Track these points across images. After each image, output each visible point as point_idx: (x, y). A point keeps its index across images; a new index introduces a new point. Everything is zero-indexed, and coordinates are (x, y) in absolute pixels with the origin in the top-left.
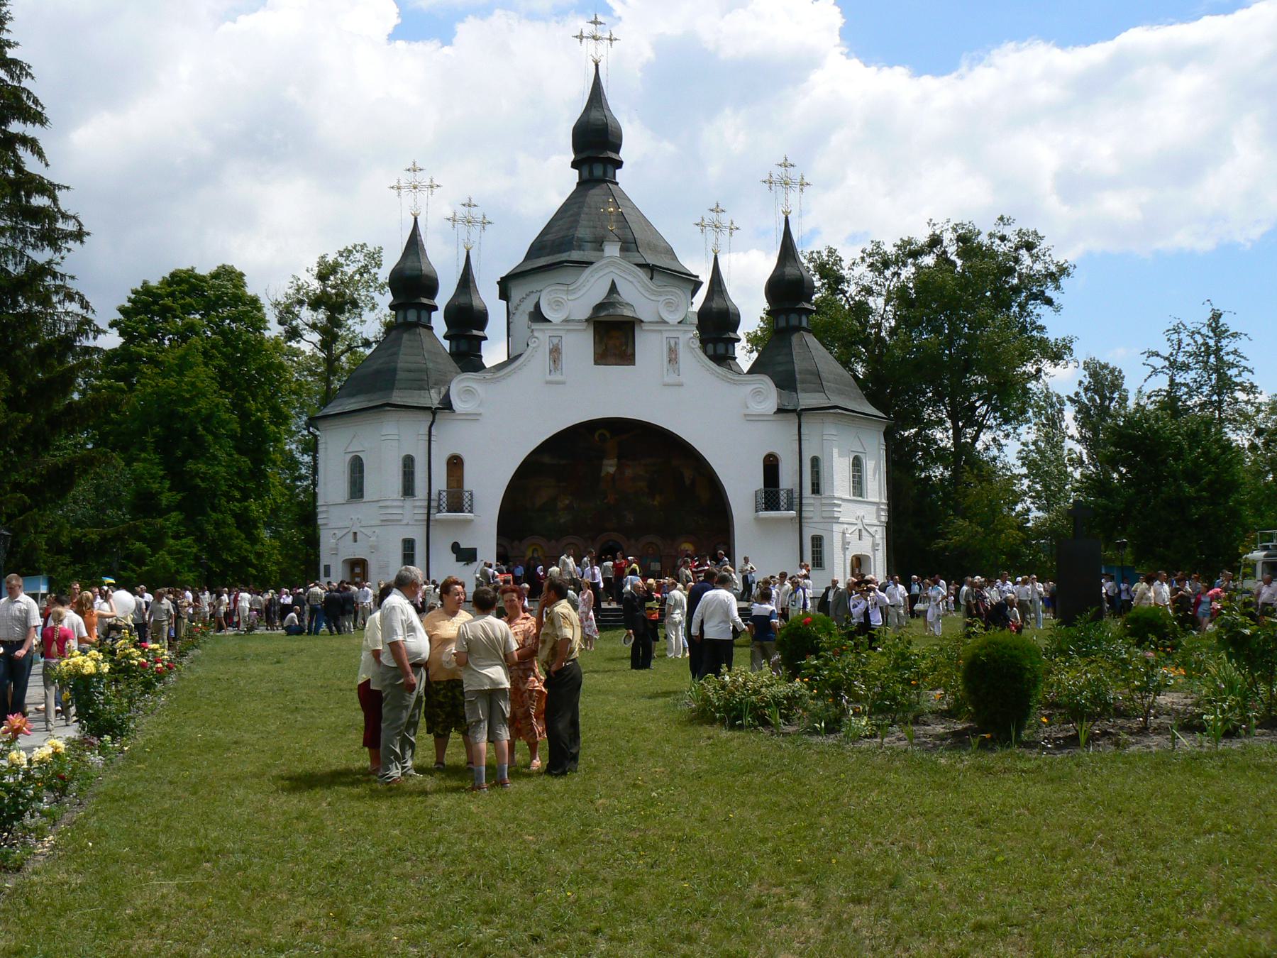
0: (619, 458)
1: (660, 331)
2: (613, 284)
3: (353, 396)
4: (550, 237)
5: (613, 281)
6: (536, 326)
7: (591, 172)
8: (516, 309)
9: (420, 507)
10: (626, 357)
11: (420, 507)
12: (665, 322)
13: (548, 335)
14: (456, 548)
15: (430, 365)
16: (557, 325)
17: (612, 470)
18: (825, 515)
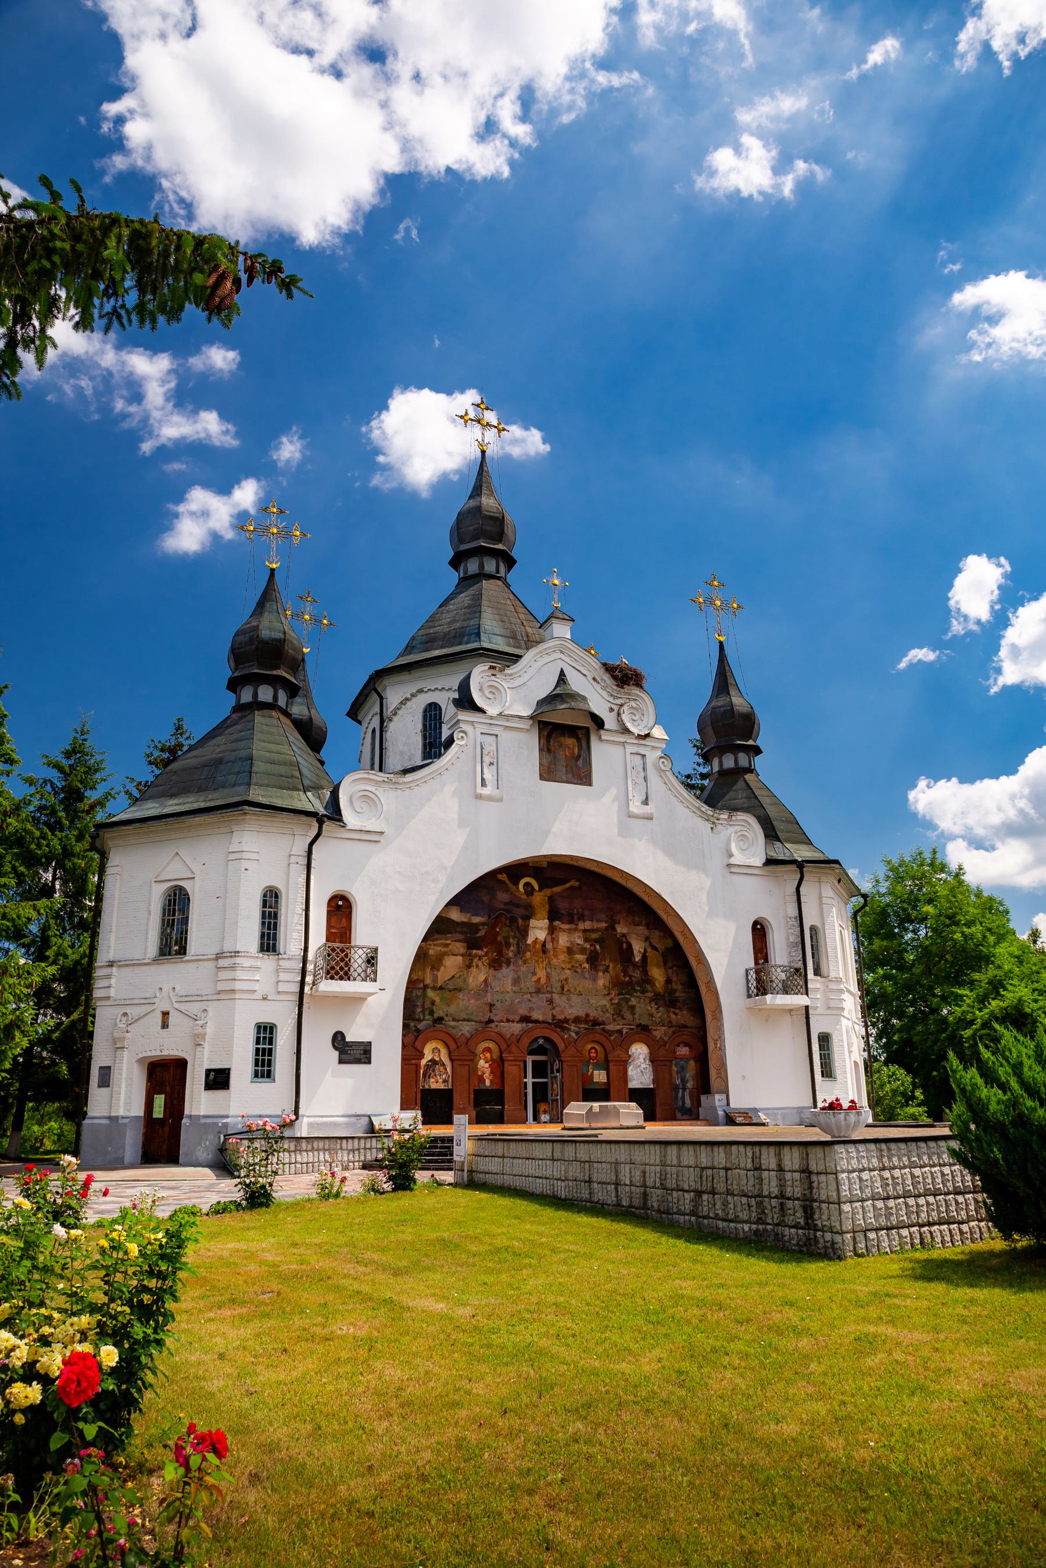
0: (551, 919)
1: (623, 744)
2: (562, 673)
3: (173, 796)
4: (442, 627)
5: (562, 671)
6: (464, 716)
7: (481, 566)
8: (395, 714)
9: (288, 970)
10: (581, 775)
11: (288, 970)
12: (626, 731)
13: (479, 731)
14: (338, 1040)
15: (299, 759)
16: (491, 718)
17: (542, 935)
18: (832, 1004)
